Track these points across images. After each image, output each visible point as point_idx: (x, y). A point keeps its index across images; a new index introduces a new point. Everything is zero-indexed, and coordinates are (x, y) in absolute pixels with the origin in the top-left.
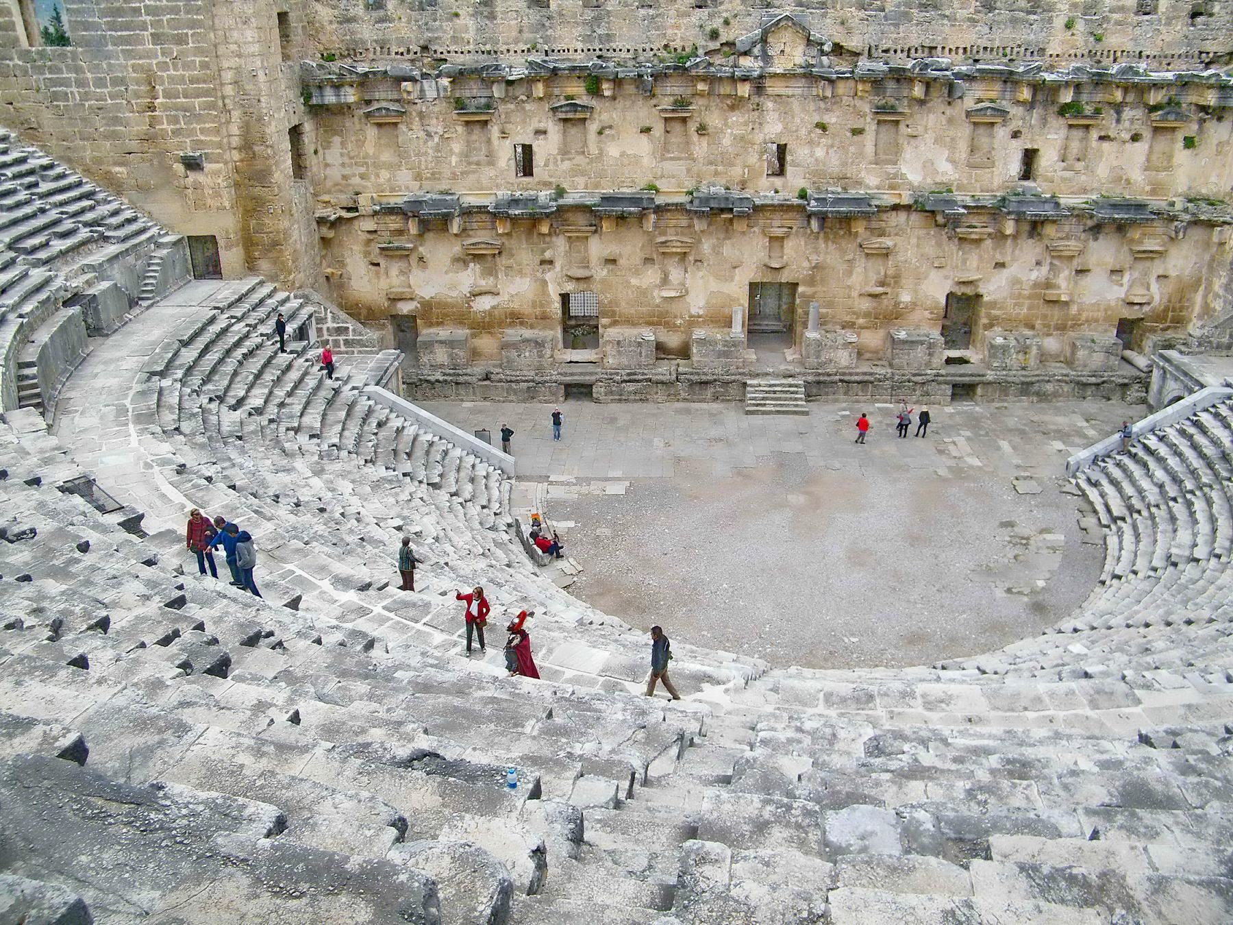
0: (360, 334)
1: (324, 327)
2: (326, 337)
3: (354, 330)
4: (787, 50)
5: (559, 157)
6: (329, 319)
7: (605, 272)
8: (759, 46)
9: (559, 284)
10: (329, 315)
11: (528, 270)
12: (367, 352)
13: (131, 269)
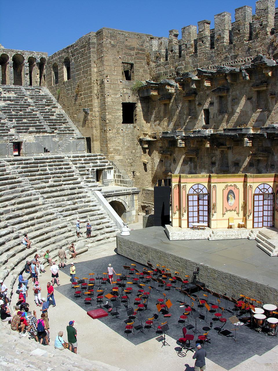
3: (122, 176)
5: (218, 115)
7: (234, 168)
11: (206, 166)
13: (55, 143)
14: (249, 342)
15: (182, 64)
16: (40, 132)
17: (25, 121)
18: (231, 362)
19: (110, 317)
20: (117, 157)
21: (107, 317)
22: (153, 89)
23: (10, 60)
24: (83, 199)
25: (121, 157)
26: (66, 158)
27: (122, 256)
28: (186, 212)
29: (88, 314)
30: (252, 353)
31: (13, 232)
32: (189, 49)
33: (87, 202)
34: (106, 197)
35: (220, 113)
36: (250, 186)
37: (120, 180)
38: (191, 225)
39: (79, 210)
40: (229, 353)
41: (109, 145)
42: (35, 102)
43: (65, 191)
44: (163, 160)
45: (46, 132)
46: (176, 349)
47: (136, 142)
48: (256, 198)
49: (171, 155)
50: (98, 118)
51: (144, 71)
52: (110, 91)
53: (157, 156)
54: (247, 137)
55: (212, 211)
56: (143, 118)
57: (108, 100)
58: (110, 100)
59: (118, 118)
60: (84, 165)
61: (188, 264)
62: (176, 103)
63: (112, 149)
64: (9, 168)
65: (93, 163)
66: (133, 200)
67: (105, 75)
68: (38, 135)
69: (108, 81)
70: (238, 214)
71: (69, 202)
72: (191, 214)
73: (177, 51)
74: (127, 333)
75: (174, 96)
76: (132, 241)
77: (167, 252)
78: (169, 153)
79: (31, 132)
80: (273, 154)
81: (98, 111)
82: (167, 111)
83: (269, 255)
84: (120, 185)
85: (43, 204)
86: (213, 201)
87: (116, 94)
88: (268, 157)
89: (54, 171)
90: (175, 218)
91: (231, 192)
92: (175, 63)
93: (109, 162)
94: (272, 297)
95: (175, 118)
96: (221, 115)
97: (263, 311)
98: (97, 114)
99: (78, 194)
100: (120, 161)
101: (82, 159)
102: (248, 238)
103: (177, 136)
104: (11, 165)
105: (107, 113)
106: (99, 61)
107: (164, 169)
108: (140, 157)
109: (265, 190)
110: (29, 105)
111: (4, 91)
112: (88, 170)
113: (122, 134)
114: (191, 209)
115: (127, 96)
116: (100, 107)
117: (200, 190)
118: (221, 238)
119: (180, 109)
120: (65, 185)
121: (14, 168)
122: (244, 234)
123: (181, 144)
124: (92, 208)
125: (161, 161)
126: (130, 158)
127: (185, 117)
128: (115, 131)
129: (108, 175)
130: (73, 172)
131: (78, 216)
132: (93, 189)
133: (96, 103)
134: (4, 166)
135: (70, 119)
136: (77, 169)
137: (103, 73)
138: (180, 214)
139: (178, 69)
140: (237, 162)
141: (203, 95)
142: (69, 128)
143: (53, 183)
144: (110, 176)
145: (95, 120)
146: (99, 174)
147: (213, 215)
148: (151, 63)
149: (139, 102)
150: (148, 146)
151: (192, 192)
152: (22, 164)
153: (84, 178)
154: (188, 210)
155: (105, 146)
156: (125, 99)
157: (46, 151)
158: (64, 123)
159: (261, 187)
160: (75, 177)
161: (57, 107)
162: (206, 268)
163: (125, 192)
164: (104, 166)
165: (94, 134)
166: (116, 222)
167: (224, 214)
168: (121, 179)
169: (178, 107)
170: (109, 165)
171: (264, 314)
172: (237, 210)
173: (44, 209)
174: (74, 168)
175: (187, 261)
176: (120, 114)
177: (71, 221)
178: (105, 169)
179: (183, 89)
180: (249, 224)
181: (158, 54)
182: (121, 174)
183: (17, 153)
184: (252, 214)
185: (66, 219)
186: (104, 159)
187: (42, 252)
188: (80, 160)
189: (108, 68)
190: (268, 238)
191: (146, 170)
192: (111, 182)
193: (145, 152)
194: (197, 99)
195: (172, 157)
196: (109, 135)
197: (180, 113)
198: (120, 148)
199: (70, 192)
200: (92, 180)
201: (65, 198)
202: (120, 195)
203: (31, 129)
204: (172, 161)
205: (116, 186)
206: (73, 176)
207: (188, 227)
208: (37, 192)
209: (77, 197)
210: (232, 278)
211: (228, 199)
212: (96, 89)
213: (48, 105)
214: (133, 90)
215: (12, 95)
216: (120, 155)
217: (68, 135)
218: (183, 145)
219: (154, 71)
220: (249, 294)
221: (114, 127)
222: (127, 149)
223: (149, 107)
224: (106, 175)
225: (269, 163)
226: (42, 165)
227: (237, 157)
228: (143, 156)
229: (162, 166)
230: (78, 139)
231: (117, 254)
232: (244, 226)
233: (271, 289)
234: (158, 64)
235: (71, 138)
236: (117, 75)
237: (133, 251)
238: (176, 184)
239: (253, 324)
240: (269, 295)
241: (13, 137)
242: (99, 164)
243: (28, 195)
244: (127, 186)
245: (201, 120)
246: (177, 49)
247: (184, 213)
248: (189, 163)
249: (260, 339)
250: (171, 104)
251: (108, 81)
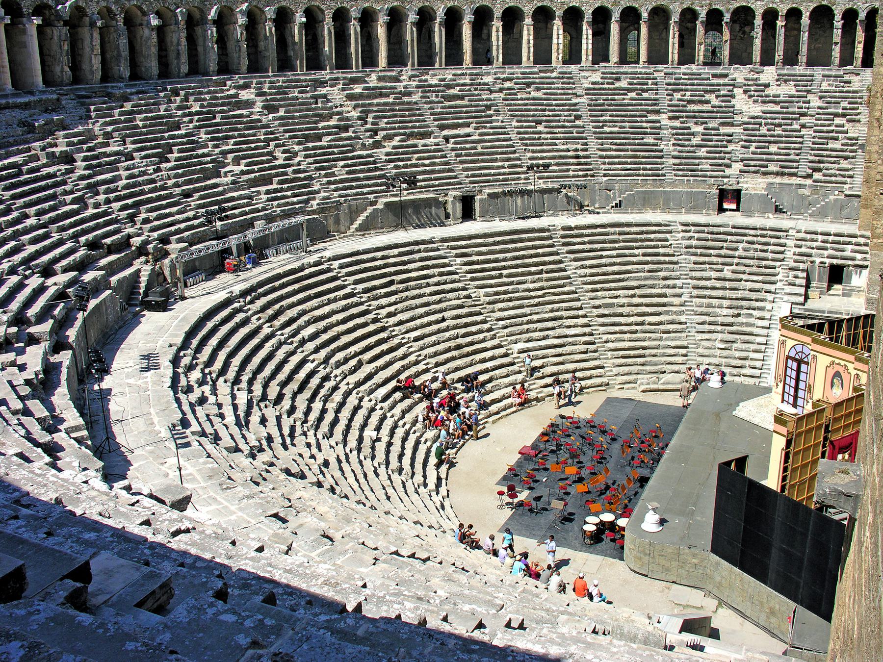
13: (803, 197)
16: (782, 174)
17: (773, 148)
23: (805, 20)
24: (756, 313)
26: (792, 232)
31: (592, 335)
33: (759, 318)
39: (734, 328)
42: (819, 108)
43: (740, 292)
45: (795, 175)
60: (814, 251)
64: (677, 239)
65: (833, 249)
68: (778, 180)
71: (725, 312)
79: (765, 174)
85: (681, 305)
89: (751, 254)
99: (757, 300)
101: (820, 237)
104: (683, 231)
110: (803, 115)
111: (777, 80)
112: (812, 262)
120: (746, 281)
121: (683, 238)
124: (756, 331)
130: (783, 260)
132: (786, 298)
134: (671, 232)
142: (847, 170)
143: (729, 275)
144: (859, 280)
146: (836, 275)
151: (792, 354)
152: (703, 232)
157: (778, 210)
158: (846, 158)
161: (859, 121)
164: (853, 259)
173: (676, 313)
174: (789, 254)
178: (849, 266)
183: (734, 206)
186: (866, 245)
187: (612, 371)
188: (813, 240)
192: (858, 291)
199: (747, 294)
200: (798, 281)
201: (726, 303)
203: (773, 167)
206: (775, 268)
208: (689, 284)
209: (747, 306)
213: (844, 115)
215: (789, 89)
224: (850, 277)
226: (734, 238)
230: (846, 195)
235: (836, 193)
241: (726, 180)
242: (848, 254)
243: (668, 287)
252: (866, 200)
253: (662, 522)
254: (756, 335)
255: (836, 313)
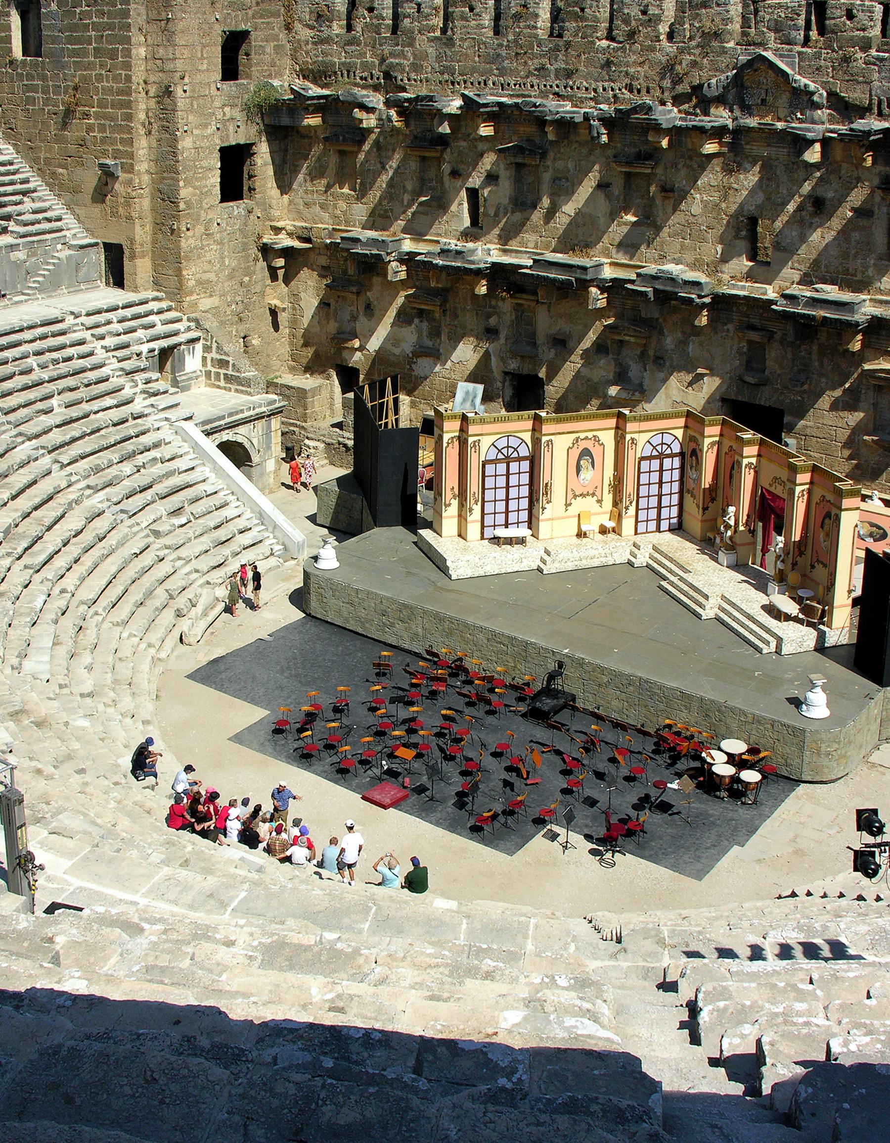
0: (238, 371)
1: (209, 357)
2: (209, 368)
3: (234, 365)
4: (770, 99)
6: (214, 349)
8: (733, 91)
9: (503, 360)
10: (214, 345)
12: (242, 392)
14: (713, 823)
15: (402, 55)
18: (699, 866)
19: (414, 798)
20: (206, 303)
21: (409, 801)
22: (311, 109)
25: (214, 301)
27: (327, 622)
28: (480, 503)
29: (364, 798)
30: (726, 843)
32: (427, 17)
34: (208, 434)
35: (516, 205)
36: (632, 439)
37: (225, 374)
38: (488, 533)
39: (159, 488)
40: (688, 848)
41: (185, 273)
43: (102, 432)
44: (333, 303)
46: (593, 852)
47: (254, 252)
48: (645, 465)
49: (358, 294)
50: (147, 190)
51: (278, 48)
52: (191, 118)
53: (311, 291)
54: (598, 287)
55: (543, 500)
56: (271, 183)
57: (186, 144)
58: (190, 145)
59: (209, 193)
61: (531, 650)
62: (379, 156)
63: (192, 283)
66: (268, 433)
67: (178, 75)
69: (185, 91)
70: (600, 501)
71: (127, 468)
72: (489, 508)
73: (388, 13)
74: (476, 831)
75: (373, 136)
76: (361, 587)
77: (470, 620)
78: (354, 289)
80: (661, 333)
81: (148, 172)
82: (346, 171)
83: (699, 616)
84: (225, 388)
86: (545, 477)
87: (205, 126)
88: (648, 338)
90: (447, 517)
91: (586, 453)
92: (381, 45)
93: (185, 318)
94: (734, 726)
95: (375, 195)
96: (520, 211)
97: (725, 758)
98: (146, 178)
100: (215, 311)
102: (630, 564)
103: (388, 254)
105: (181, 184)
106: (153, 28)
107: (332, 327)
108: (263, 293)
109: (665, 447)
113: (217, 237)
114: (489, 495)
115: (231, 128)
116: (156, 161)
117: (511, 450)
118: (570, 566)
119: (391, 173)
122: (616, 551)
123: (397, 271)
125: (324, 305)
126: (238, 299)
127: (406, 198)
128: (200, 229)
129: (188, 359)
131: (162, 508)
133: (143, 147)
135: (39, 176)
136: (110, 354)
137: (170, 66)
138: (462, 506)
139: (391, 66)
140: (561, 337)
141: (466, 151)
144: (193, 362)
145: (141, 196)
147: (544, 508)
148: (298, 26)
149: (264, 139)
150: (285, 263)
153: (140, 383)
154: (483, 498)
155: (170, 272)
156: (228, 135)
159: (657, 440)
160: (115, 382)
162: (581, 663)
163: (252, 413)
164: (176, 334)
165: (137, 237)
166: (261, 514)
167: (568, 505)
168: (230, 372)
169: (384, 168)
170: (189, 329)
171: (727, 763)
172: (598, 493)
175: (527, 644)
176: (215, 179)
177: (151, 527)
179: (407, 125)
180: (628, 524)
181: (325, 8)
182: (230, 359)
184: (634, 503)
185: (138, 524)
189: (186, 53)
190: (681, 567)
191: (276, 326)
192: (197, 378)
193: (274, 277)
194: (447, 157)
195: (362, 298)
196: (187, 242)
197: (390, 184)
198: (212, 276)
202: (238, 425)
204: (362, 312)
205: (208, 389)
207: (482, 538)
210: (646, 689)
211: (578, 470)
212: (143, 107)
214: (247, 108)
216: (211, 296)
217: (48, 236)
218: (403, 275)
219: (307, 53)
220: (681, 719)
221: (199, 216)
222: (231, 277)
223: (286, 151)
224: (182, 360)
225: (651, 352)
227: (562, 326)
228: (268, 291)
229: (328, 320)
231: (309, 615)
232: (617, 531)
233: (732, 710)
234: (323, 36)
236: (208, 70)
237: (363, 613)
238: (453, 435)
239: (708, 782)
240: (729, 720)
242: (160, 329)
244: (250, 394)
245: (458, 216)
246: (388, 8)
247: (474, 507)
248: (416, 321)
249: (731, 814)
250: (361, 156)
251: (185, 91)
252: (142, 245)
253: (797, 703)
254: (191, 486)
255: (237, 413)
